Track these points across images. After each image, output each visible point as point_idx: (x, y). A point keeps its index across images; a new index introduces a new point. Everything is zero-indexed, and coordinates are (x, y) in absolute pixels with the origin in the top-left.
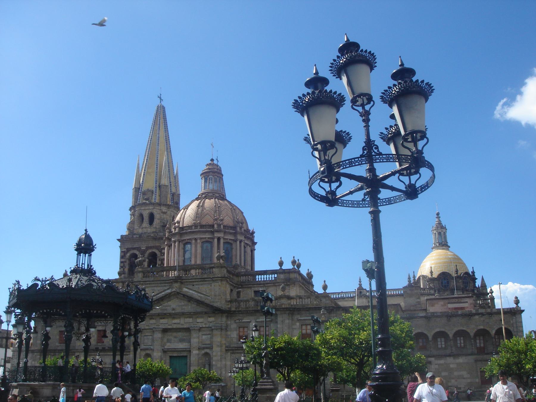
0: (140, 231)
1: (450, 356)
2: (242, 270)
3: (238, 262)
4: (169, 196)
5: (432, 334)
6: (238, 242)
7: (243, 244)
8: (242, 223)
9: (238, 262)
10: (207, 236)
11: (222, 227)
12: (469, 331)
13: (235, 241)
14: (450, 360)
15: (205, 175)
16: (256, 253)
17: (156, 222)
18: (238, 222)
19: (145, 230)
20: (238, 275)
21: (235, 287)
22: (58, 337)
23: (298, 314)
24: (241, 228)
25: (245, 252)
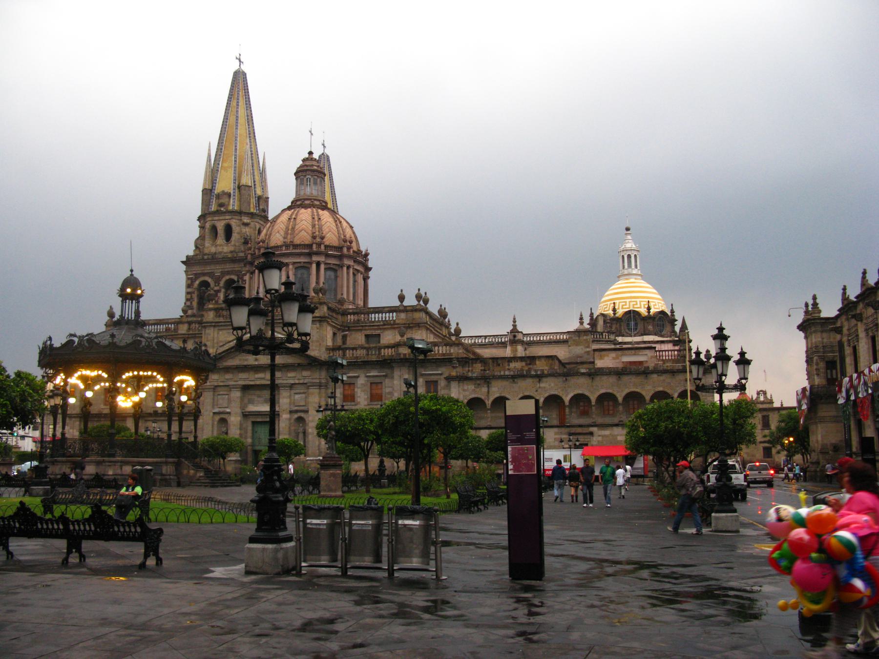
0: (213, 250)
1: (617, 425)
2: (351, 307)
3: (345, 296)
4: (253, 201)
5: (596, 396)
6: (345, 269)
7: (351, 270)
8: (351, 242)
9: (345, 296)
10: (302, 260)
11: (323, 247)
12: (644, 393)
13: (341, 266)
15: (300, 174)
16: (370, 281)
17: (235, 236)
18: (345, 241)
19: (220, 249)
20: (345, 313)
21: (339, 329)
23: (422, 367)
24: (349, 248)
25: (355, 281)
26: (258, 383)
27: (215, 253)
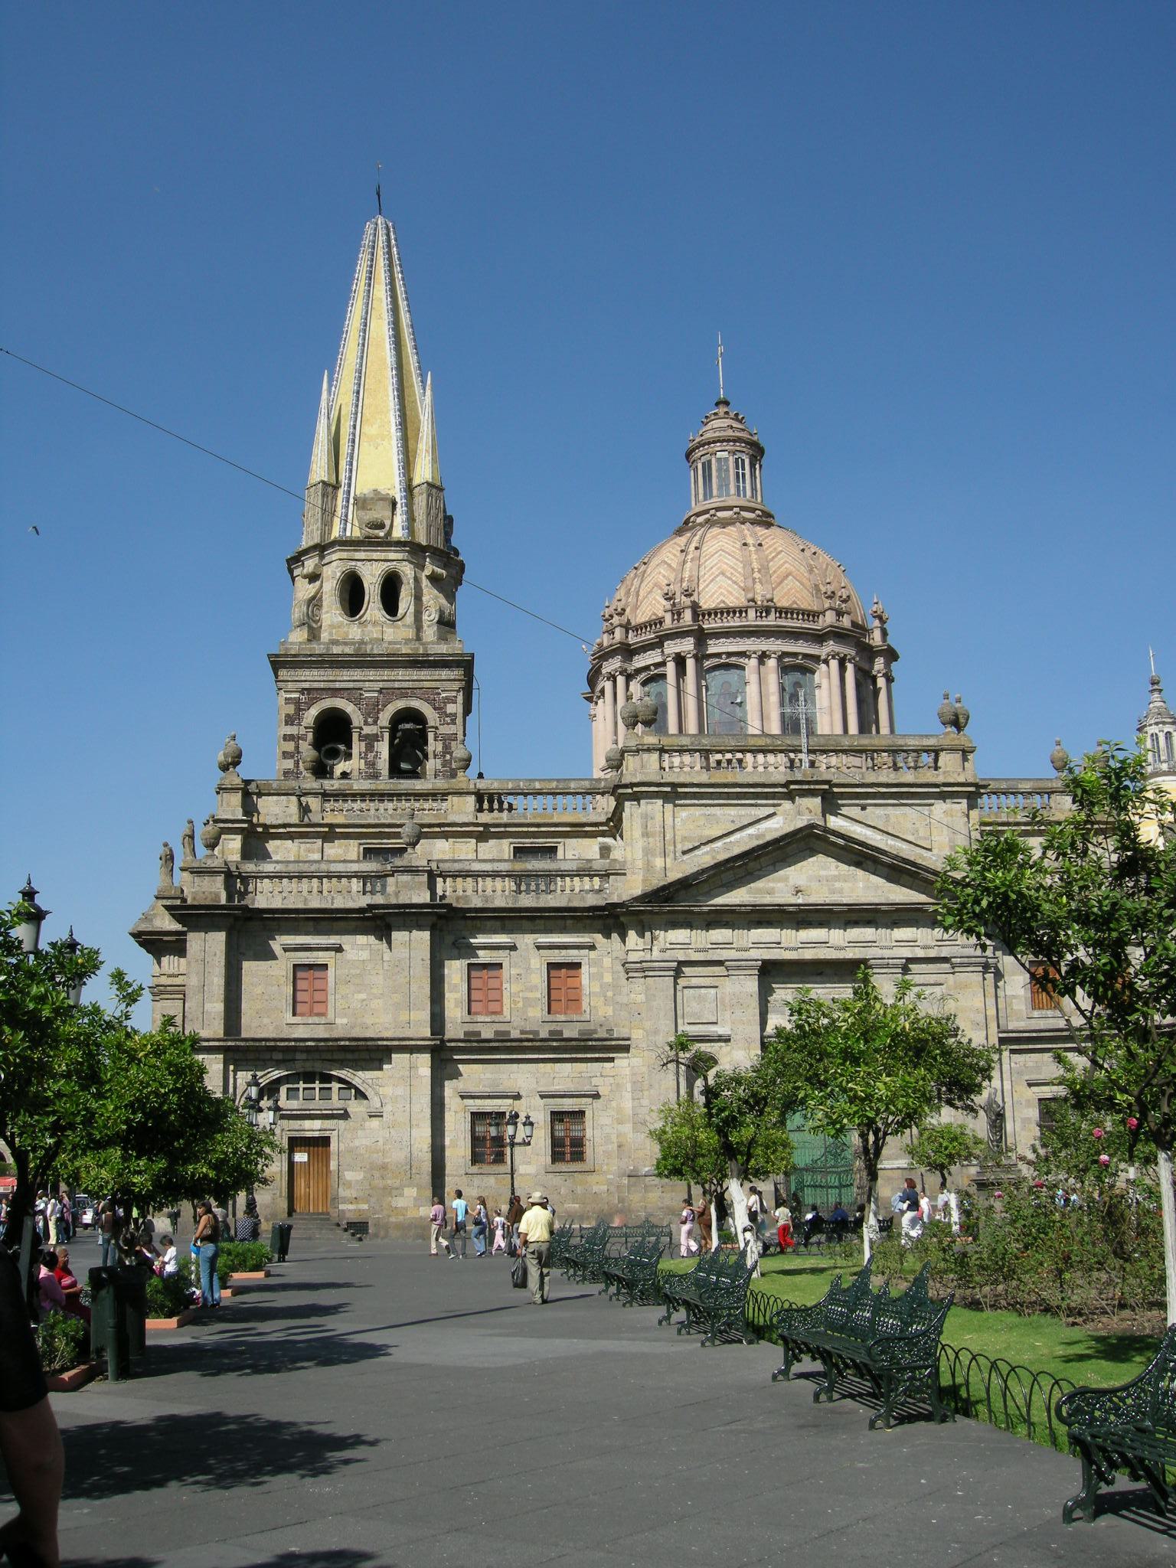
0: (354, 632)
10: (801, 647)
19: (374, 633)
26: (808, 955)
27: (362, 642)
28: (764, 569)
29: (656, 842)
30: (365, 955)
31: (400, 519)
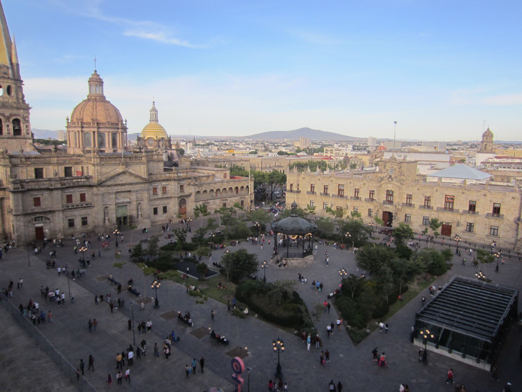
10: (115, 130)
14: (233, 198)
22: (33, 202)
28: (109, 115)
29: (99, 174)
30: (47, 195)
31: (10, 72)
